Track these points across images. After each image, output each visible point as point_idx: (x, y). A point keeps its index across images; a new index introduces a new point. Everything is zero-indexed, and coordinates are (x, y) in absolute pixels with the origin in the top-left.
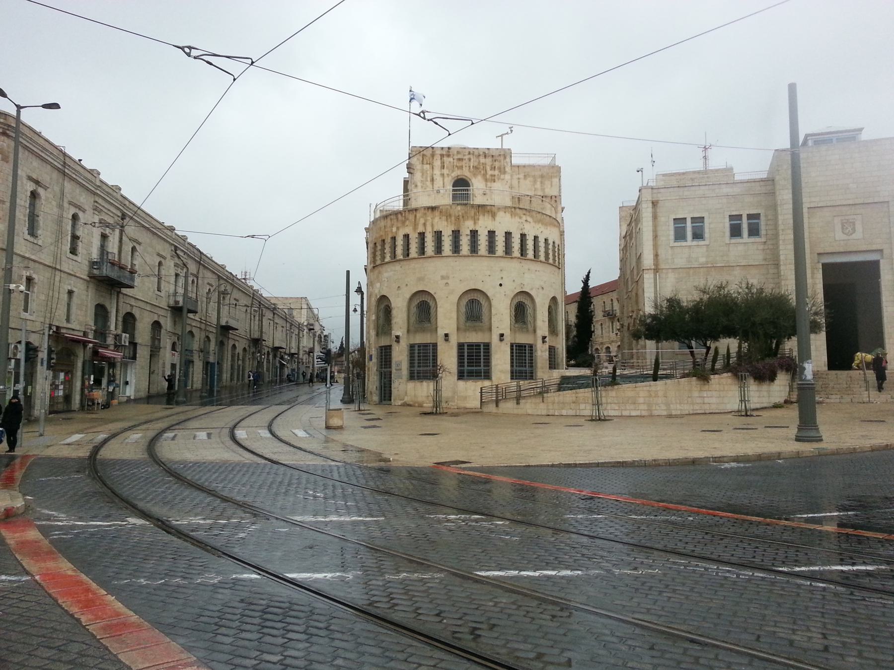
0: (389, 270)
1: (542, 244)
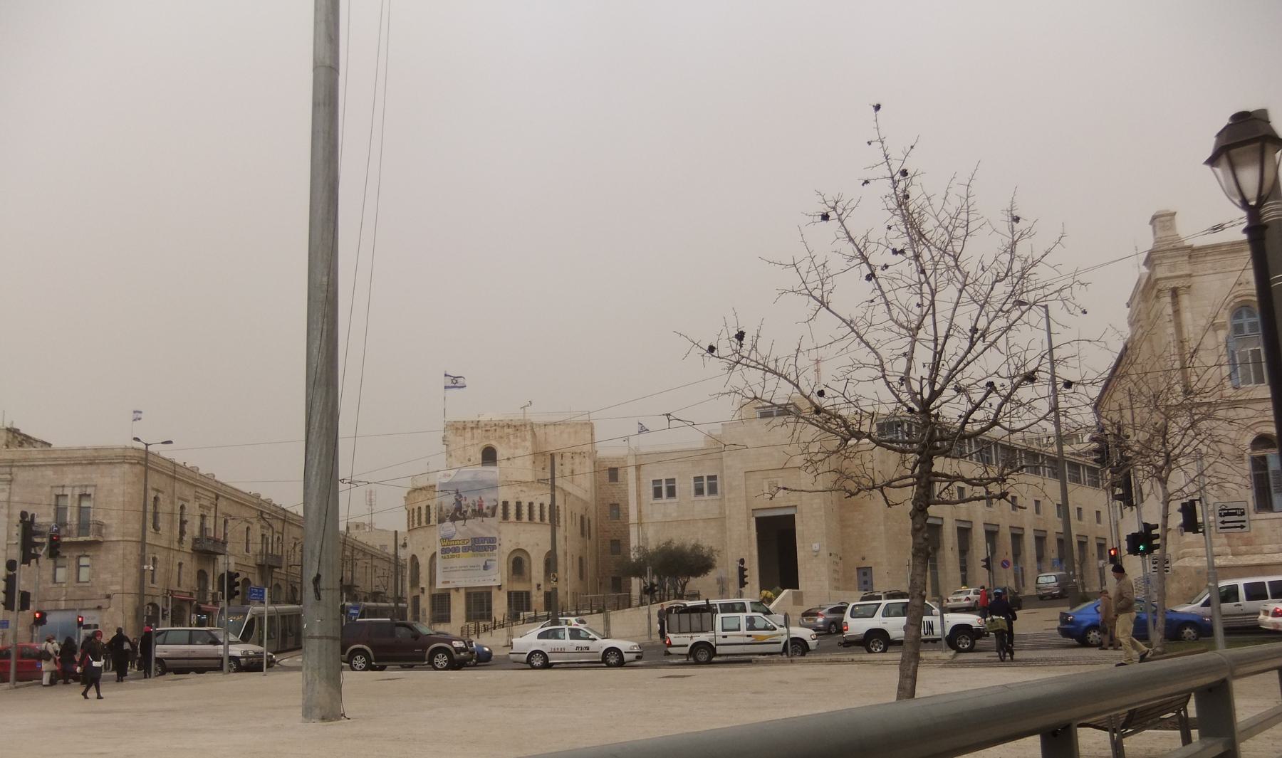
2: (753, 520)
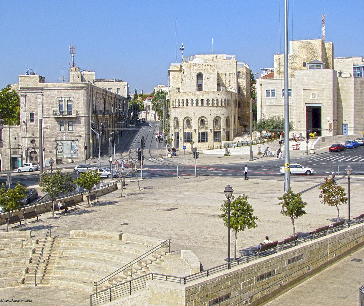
0: (178, 109)
1: (223, 100)
2: (305, 107)
